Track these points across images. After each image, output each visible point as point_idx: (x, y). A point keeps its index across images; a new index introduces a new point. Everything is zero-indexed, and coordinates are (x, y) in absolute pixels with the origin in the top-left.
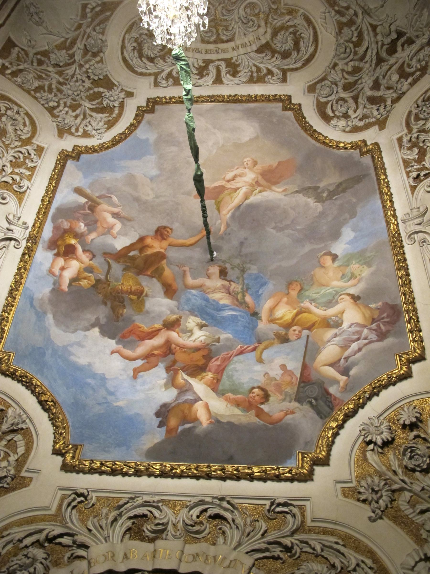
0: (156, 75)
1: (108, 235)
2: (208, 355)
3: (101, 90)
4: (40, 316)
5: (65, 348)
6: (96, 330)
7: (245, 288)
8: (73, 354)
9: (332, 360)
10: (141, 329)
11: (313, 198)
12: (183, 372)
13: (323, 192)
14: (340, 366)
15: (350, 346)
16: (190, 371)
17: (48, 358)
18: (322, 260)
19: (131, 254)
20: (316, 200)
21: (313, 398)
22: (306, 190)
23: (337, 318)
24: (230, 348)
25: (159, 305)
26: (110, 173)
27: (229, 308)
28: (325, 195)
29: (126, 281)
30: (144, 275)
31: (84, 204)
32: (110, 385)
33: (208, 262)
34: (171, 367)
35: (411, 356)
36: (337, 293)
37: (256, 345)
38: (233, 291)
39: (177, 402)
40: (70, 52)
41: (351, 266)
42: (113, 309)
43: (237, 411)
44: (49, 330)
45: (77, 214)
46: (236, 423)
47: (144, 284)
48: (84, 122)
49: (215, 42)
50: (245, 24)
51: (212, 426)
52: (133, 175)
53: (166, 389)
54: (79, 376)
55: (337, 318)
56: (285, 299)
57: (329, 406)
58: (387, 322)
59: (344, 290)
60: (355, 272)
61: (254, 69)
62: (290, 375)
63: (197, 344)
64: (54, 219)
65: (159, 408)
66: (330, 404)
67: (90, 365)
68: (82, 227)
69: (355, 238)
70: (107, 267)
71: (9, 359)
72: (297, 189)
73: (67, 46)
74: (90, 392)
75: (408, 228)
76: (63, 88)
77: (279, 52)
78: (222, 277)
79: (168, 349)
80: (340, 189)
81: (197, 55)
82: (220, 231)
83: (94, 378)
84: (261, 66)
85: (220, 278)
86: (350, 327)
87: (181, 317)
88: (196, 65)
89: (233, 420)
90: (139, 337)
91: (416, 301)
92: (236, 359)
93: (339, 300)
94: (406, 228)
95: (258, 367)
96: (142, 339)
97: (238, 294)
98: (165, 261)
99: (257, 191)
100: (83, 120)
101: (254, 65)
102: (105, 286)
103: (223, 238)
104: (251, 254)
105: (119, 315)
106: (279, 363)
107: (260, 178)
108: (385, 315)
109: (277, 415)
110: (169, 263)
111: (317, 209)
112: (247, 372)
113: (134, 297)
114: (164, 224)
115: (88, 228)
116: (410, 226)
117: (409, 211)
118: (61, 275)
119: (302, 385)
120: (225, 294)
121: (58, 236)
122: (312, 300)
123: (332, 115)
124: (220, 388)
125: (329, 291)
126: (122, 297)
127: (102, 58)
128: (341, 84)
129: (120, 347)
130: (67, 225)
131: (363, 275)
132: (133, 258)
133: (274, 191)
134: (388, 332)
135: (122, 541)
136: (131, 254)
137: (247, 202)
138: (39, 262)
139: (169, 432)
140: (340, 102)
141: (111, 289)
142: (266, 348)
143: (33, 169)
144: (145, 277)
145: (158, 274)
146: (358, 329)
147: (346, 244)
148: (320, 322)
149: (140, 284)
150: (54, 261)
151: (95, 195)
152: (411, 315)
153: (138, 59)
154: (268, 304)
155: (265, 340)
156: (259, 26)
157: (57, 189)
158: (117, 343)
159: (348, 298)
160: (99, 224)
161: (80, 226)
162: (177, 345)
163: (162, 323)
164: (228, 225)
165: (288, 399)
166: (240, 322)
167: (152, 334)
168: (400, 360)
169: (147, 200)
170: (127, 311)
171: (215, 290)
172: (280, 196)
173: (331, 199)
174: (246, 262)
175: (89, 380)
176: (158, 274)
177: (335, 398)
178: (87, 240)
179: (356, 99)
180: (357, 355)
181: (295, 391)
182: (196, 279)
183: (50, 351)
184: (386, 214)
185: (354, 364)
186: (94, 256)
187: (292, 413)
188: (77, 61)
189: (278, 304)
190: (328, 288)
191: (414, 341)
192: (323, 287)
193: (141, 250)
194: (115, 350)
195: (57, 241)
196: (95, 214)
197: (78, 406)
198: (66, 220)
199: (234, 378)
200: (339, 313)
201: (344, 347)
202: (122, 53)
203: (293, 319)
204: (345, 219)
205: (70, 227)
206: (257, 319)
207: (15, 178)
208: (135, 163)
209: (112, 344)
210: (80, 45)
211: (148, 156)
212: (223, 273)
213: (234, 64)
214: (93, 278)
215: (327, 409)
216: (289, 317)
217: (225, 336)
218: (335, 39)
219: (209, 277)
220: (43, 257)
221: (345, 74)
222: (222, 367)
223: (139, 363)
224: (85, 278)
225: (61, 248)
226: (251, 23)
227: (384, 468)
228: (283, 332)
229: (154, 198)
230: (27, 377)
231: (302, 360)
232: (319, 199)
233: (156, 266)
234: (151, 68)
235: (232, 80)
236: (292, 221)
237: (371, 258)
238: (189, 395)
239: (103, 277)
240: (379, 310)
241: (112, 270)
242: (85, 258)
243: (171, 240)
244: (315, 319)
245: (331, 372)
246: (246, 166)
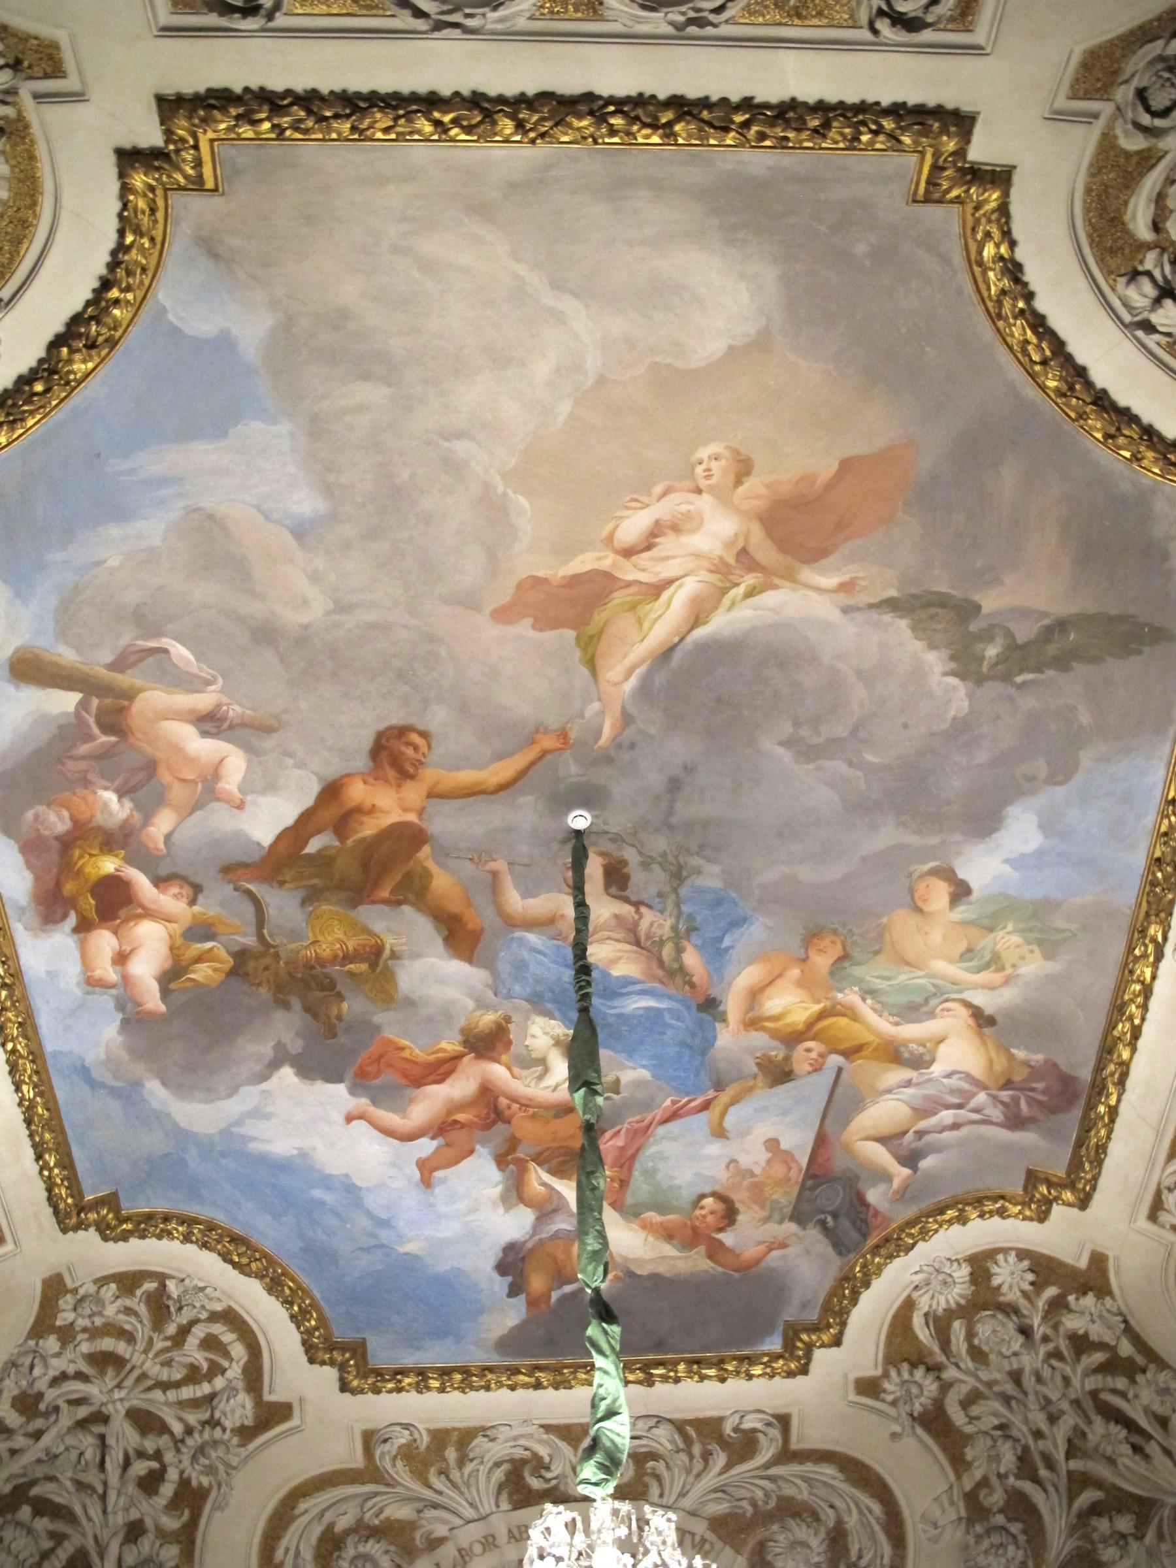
1: (214, 805)
5: (226, 1133)
6: (287, 1073)
8: (254, 1139)
9: (885, 1131)
10: (406, 1054)
11: (945, 653)
12: (539, 1165)
13: (987, 636)
14: (901, 1144)
15: (936, 1114)
16: (555, 1162)
17: (194, 1162)
18: (921, 887)
20: (953, 665)
21: (828, 1212)
22: (928, 605)
23: (921, 1050)
24: (647, 1106)
25: (439, 981)
26: (114, 531)
27: (638, 987)
28: (992, 651)
29: (322, 932)
30: (373, 902)
31: (77, 714)
32: (372, 1202)
34: (507, 1153)
36: (939, 992)
37: (711, 1094)
39: (537, 1238)
41: (1001, 933)
43: (668, 1250)
44: (168, 1115)
45: (72, 765)
46: (668, 1275)
47: (379, 927)
51: (620, 1285)
52: (211, 517)
53: (508, 1208)
54: (285, 1181)
55: (921, 1050)
56: (795, 972)
57: (859, 1230)
58: (1039, 1103)
59: (961, 992)
60: (1004, 955)
62: (786, 1162)
65: (501, 1255)
66: (864, 1226)
68: (111, 806)
69: (1040, 853)
70: (249, 910)
72: (893, 593)
74: (333, 1222)
78: (613, 890)
79: (491, 1108)
80: (1052, 649)
83: (329, 1188)
85: (608, 894)
86: (949, 1076)
87: (508, 1019)
89: (661, 1269)
90: (406, 1076)
92: (661, 1130)
93: (938, 1010)
95: (715, 1149)
96: (418, 1082)
98: (426, 850)
99: (741, 590)
102: (264, 962)
104: (706, 824)
105: (334, 1020)
106: (767, 1132)
107: (757, 533)
108: (1040, 1085)
109: (750, 1252)
110: (443, 854)
111: (950, 700)
112: (687, 1159)
113: (363, 967)
114: (396, 720)
115: (132, 800)
118: (126, 979)
119: (810, 1183)
120: (627, 947)
121: (55, 871)
122: (868, 992)
123: (1142, 230)
124: (629, 1200)
125: (921, 981)
126: (326, 976)
129: (363, 1102)
130: (60, 818)
132: (323, 860)
135: (498, 1506)
137: (700, 633)
138: (43, 975)
139: (532, 1303)
141: (287, 963)
142: (735, 1101)
145: (414, 891)
146: (966, 1086)
147: (1006, 861)
148: (876, 1049)
149: (367, 931)
150: (83, 948)
151: (98, 661)
154: (746, 977)
155: (732, 1081)
158: (353, 1091)
159: (964, 1012)
160: (165, 777)
161: (106, 805)
162: (513, 1099)
163: (460, 1038)
164: (627, 719)
165: (777, 1216)
166: (670, 1032)
169: (306, 627)
170: (352, 1006)
172: (824, 608)
173: (1007, 678)
174: (688, 850)
175: (318, 1193)
177: (876, 1214)
178: (151, 845)
180: (947, 1135)
181: (793, 1201)
182: (535, 896)
183: (194, 1151)
186: (197, 889)
187: (783, 1246)
189: (771, 983)
190: (921, 973)
192: (907, 968)
194: (355, 1113)
195: (58, 885)
196: (132, 740)
197: (319, 1256)
198: (49, 805)
199: (659, 1176)
200: (930, 1040)
201: (922, 1111)
203: (810, 1025)
204: (1031, 779)
206: (715, 1019)
208: (201, 455)
211: (257, 425)
214: (223, 954)
215: (855, 1235)
222: (630, 1153)
223: (426, 1146)
224: (199, 959)
225: (82, 903)
227: (936, 1349)
229: (329, 613)
231: (817, 1126)
232: (966, 666)
233: (405, 869)
236: (854, 732)
237: (1064, 935)
238: (563, 1221)
239: (250, 941)
241: (271, 912)
242: (171, 901)
243: (431, 775)
244: (868, 1037)
245: (880, 1155)
246: (703, 483)
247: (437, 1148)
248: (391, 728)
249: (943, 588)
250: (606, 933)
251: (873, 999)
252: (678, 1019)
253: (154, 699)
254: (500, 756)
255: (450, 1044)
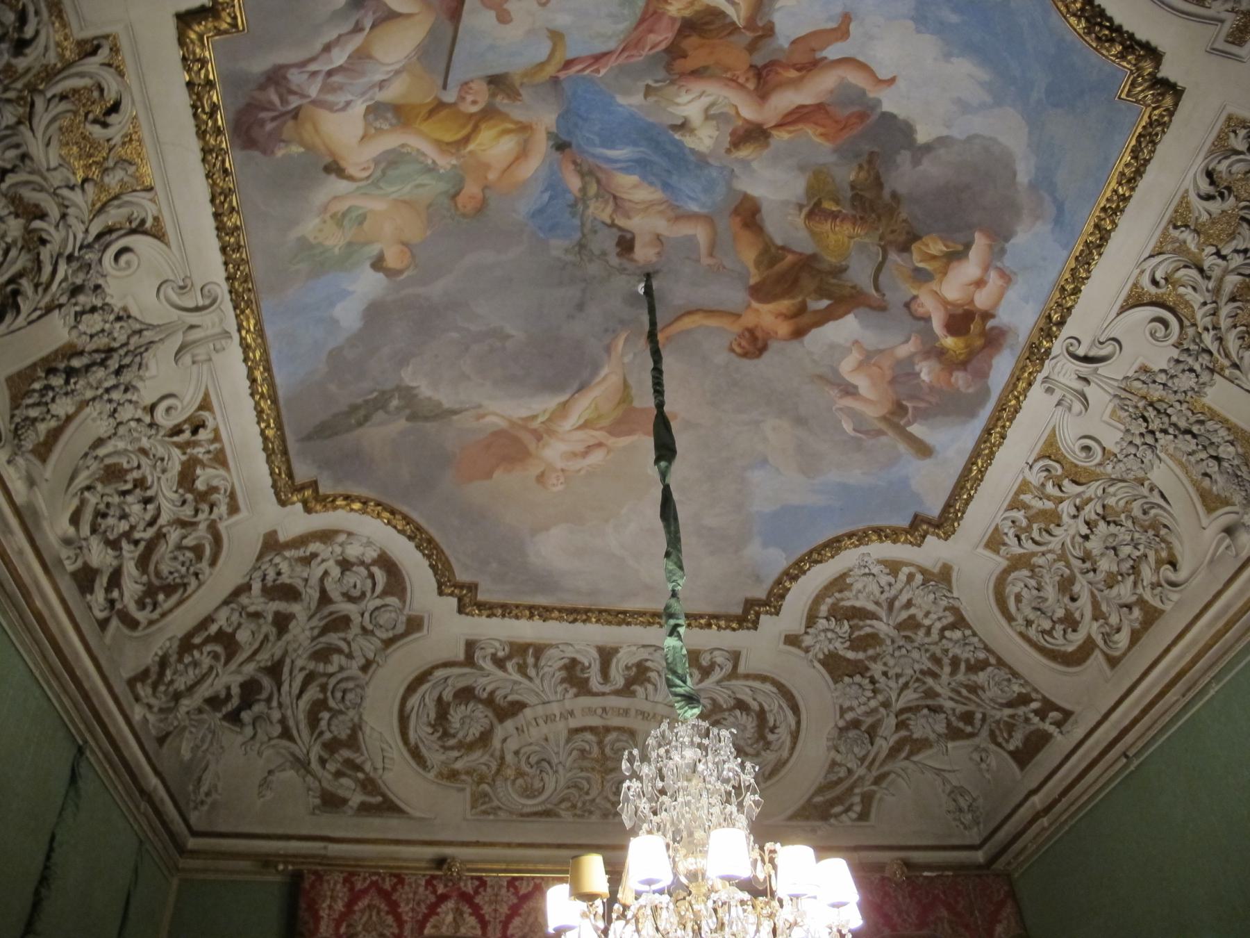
0: (734, 674)
2: (674, 59)
3: (850, 655)
4: (1044, 182)
6: (922, 137)
7: (580, 207)
10: (821, 130)
12: (733, 23)
13: (399, 409)
15: (350, 57)
19: (825, 303)
20: (415, 392)
23: (378, 124)
25: (774, 184)
27: (619, 165)
28: (395, 403)
30: (801, 254)
31: (915, 421)
33: (657, 272)
34: (761, 37)
35: (210, 25)
37: (562, 75)
38: (607, 202)
40: (903, 733)
41: (342, 243)
42: (878, 184)
47: (803, 234)
48: (893, 592)
49: (608, 730)
50: (544, 760)
56: (492, 176)
58: (265, 109)
59: (358, 188)
61: (531, 672)
63: (697, 86)
64: (986, 392)
67: (947, 56)
68: (926, 372)
70: (882, 278)
71: (1133, 85)
72: (455, 417)
73: (909, 746)
75: (217, 320)
76: (928, 664)
77: (480, 701)
78: (629, 236)
79: (763, 79)
80: (362, 412)
81: (647, 707)
82: (627, 340)
84: (517, 677)
85: (633, 234)
86: (348, 104)
87: (728, 151)
88: (650, 687)
90: (827, 112)
91: (199, 155)
92: (612, 45)
94: (221, 321)
95: (562, 20)
96: (820, 107)
97: (597, 196)
98: (752, 281)
99: (540, 419)
100: (896, 598)
101: (530, 679)
102: (891, 237)
103: (622, 322)
105: (866, 166)
107: (532, 446)
114: (746, 363)
116: (213, 326)
117: (215, 357)
118: (986, 269)
120: (625, 196)
122: (431, 169)
123: (375, 569)
126: (854, 207)
127: (842, 716)
128: (355, 629)
131: (317, 221)
132: (821, 293)
133: (503, 417)
134: (262, 87)
136: (825, 303)
137: (563, 398)
140: (356, 593)
141: (877, 229)
142: (541, 66)
143: (1015, 504)
144: (799, 250)
145: (770, 254)
146: (330, 98)
149: (813, 234)
150: (996, 304)
151: (890, 438)
152: (210, 123)
153: (766, 707)
156: (517, 753)
157: (970, 458)
158: (878, 102)
159: (351, 170)
160: (889, 374)
161: (929, 373)
162: (742, 86)
163: (771, 140)
164: (608, 349)
167: (798, 116)
168: (235, 18)
170: (847, 174)
171: (647, 208)
173: (383, 393)
175: (954, 18)
176: (770, 254)
179: (325, 598)
180: (334, 35)
184: (265, 352)
185: (338, 15)
186: (907, 305)
188: (892, 716)
189: (509, 166)
190: (394, 196)
191: (203, 62)
193: (802, 310)
195: (984, 347)
198: (958, 389)
201: (362, 56)
202: (798, 723)
203: (476, 129)
205: (951, 375)
207: (1057, 489)
209: (890, 102)
210: (883, 745)
212: (626, 245)
213: (573, 685)
214: (916, 256)
216: (486, 135)
217: (631, 101)
218: (365, 717)
219: (658, 238)
220: (1019, 314)
221: (346, 650)
222: (644, 26)
224: (934, 258)
226: (533, 760)
228: (501, 102)
230: (1098, 39)
232: (408, 394)
234: (742, 689)
235: (578, 652)
239: (893, 256)
240: (284, 137)
241: (870, 271)
242: (927, 303)
243: (736, 328)
244: (425, 127)
246: (560, 473)
247: (823, 49)
248: (751, 358)
249: (428, 425)
250: (638, 207)
251: (427, 165)
252: (588, 139)
253: (872, 413)
254: (688, 332)
255: (781, 137)
